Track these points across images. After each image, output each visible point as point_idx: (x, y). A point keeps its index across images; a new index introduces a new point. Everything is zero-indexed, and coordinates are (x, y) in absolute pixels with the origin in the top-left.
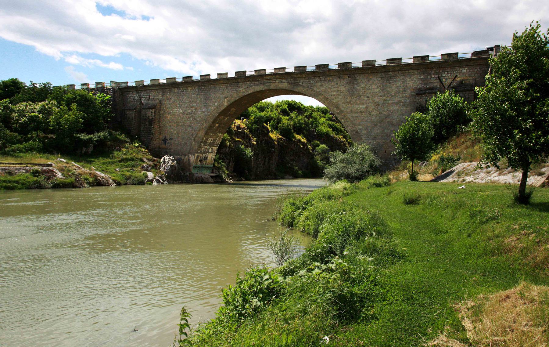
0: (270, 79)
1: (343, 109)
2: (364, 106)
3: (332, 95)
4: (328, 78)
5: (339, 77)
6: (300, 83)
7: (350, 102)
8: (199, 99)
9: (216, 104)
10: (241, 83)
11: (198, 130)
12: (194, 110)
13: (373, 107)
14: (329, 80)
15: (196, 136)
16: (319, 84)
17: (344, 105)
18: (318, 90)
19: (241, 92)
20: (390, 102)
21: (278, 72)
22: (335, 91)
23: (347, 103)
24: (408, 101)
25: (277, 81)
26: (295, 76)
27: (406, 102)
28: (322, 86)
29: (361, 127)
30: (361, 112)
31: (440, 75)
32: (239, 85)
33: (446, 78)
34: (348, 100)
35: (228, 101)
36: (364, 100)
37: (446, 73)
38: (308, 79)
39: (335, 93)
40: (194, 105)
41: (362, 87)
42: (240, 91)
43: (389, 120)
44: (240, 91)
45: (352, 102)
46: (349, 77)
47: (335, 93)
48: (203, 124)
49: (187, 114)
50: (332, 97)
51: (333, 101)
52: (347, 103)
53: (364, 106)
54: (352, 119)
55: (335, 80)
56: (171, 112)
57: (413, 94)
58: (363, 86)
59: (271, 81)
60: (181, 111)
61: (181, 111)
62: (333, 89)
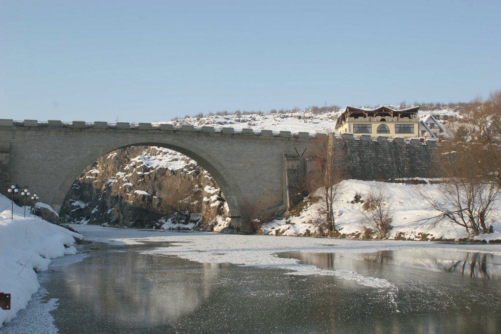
3: (214, 153)
9: (89, 152)
12: (59, 157)
19: (120, 142)
29: (240, 182)
30: (240, 170)
34: (229, 159)
40: (58, 151)
41: (240, 149)
49: (49, 161)
50: (215, 155)
56: (26, 156)
57: (279, 158)
59: (154, 136)
60: (41, 157)
61: (41, 157)
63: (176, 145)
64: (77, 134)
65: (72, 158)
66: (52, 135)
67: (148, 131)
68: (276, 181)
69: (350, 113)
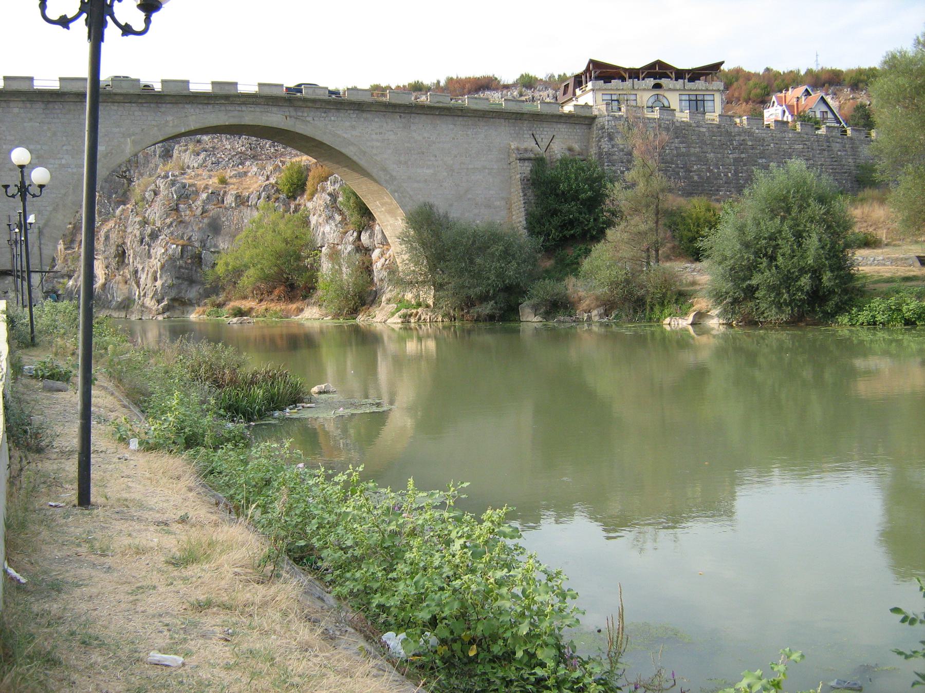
0: (244, 103)
1: (394, 174)
2: (431, 171)
3: (372, 147)
4: (364, 115)
5: (384, 115)
6: (309, 119)
7: (406, 163)
8: (49, 135)
10: (169, 106)
11: (50, 209)
13: (445, 174)
14: (366, 119)
15: (46, 225)
16: (348, 124)
17: (395, 166)
18: (346, 136)
19: (171, 125)
20: (470, 166)
21: (267, 92)
22: (378, 141)
23: (400, 163)
24: (495, 167)
25: (258, 109)
26: (300, 103)
27: (492, 169)
28: (353, 127)
30: (426, 181)
31: (534, 133)
32: (163, 110)
33: (542, 136)
34: (402, 159)
35: (134, 142)
36: (430, 160)
37: (541, 129)
38: (325, 112)
39: (378, 144)
41: (424, 138)
42: (167, 122)
43: (470, 196)
44: (167, 122)
45: (409, 163)
46: (400, 117)
47: (378, 144)
48: (65, 195)
50: (375, 151)
51: (375, 157)
52: (400, 163)
53: (429, 171)
54: (411, 193)
55: (376, 120)
57: (502, 156)
58: (426, 135)
59: (244, 108)
62: (374, 136)
63: (292, 130)
64: (72, 107)
65: (64, 162)
66: (16, 110)
67: (231, 99)
68: (498, 203)
69: (595, 72)
